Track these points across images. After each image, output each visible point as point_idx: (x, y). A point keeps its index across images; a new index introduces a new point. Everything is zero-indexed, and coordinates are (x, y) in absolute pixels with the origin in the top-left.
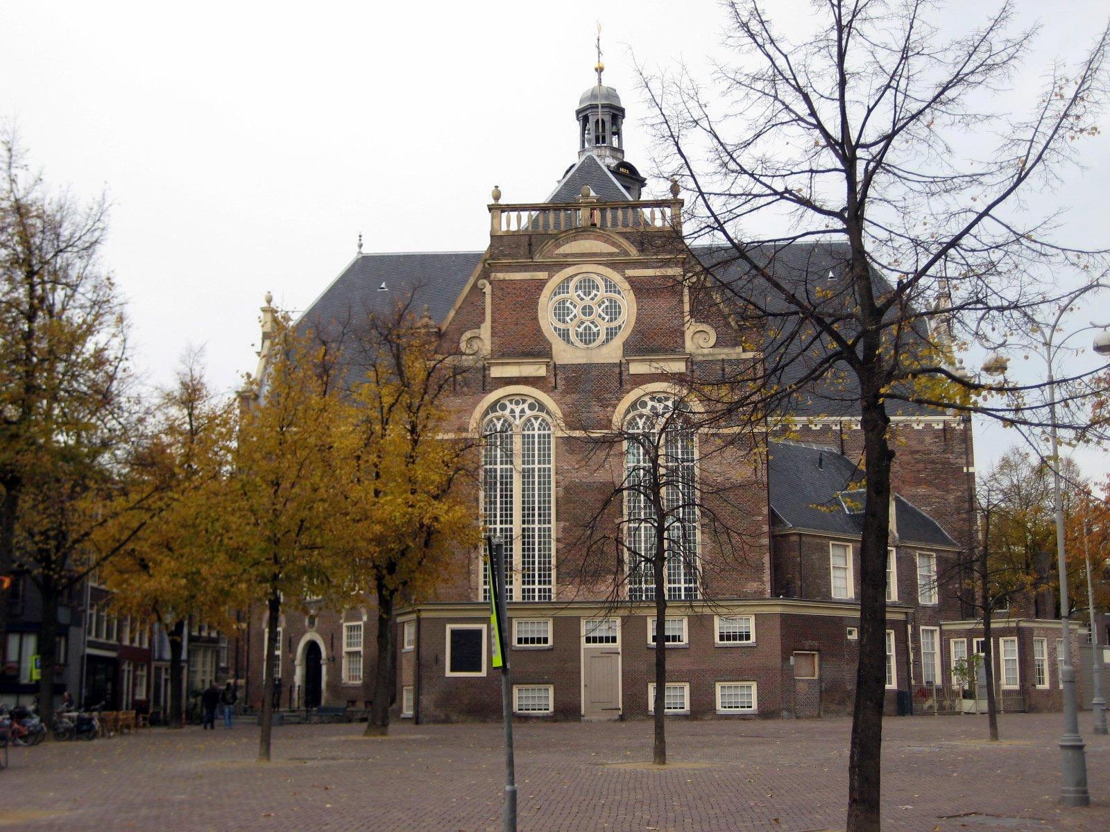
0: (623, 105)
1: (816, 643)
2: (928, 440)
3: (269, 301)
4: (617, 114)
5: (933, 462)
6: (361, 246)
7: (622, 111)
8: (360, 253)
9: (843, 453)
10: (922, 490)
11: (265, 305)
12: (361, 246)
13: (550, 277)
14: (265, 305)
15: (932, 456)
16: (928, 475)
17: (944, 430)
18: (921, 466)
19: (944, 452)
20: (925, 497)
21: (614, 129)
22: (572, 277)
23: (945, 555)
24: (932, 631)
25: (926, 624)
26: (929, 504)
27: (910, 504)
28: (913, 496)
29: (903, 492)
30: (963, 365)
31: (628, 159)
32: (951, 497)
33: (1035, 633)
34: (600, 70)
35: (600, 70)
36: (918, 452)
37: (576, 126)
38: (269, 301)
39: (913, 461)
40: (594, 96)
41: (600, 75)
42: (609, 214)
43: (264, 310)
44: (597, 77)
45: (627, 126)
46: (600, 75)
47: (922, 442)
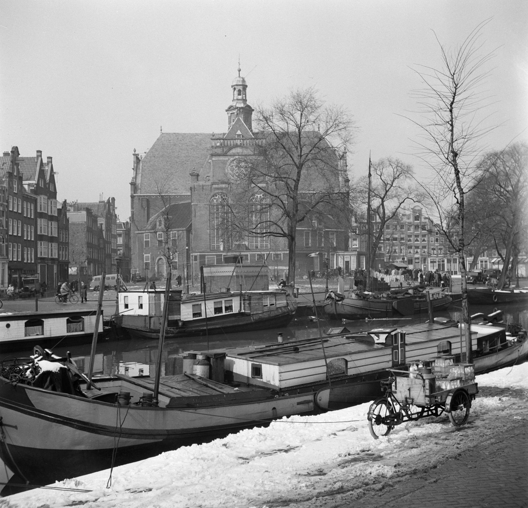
0: (247, 84)
3: (135, 151)
4: (245, 87)
6: (161, 130)
7: (247, 86)
11: (134, 153)
12: (161, 130)
14: (134, 153)
21: (244, 93)
22: (235, 159)
31: (248, 103)
34: (239, 71)
35: (239, 71)
37: (232, 90)
38: (135, 151)
42: (245, 141)
43: (134, 155)
45: (248, 90)
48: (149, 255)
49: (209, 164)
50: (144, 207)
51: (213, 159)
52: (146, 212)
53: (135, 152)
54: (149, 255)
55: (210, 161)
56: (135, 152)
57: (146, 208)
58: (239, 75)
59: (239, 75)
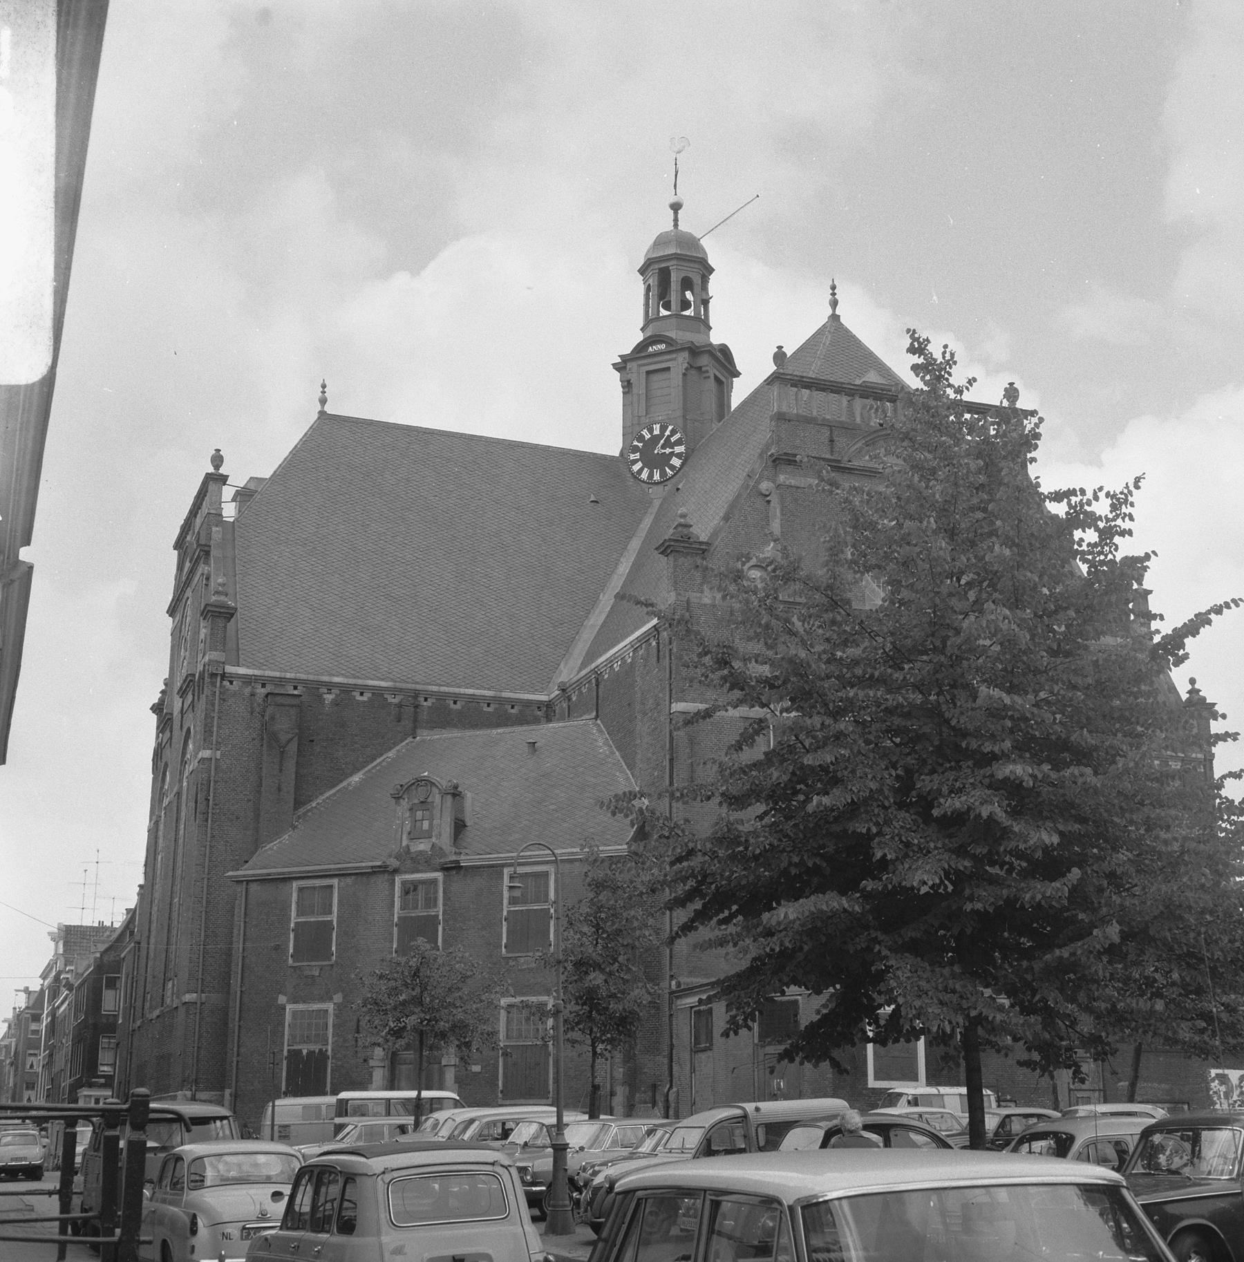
6: (323, 401)
7: (711, 270)
8: (322, 413)
12: (323, 401)
30: (1197, 686)
34: (676, 207)
35: (676, 207)
40: (660, 241)
41: (676, 213)
44: (672, 217)
46: (676, 213)
48: (330, 1007)
49: (759, 504)
50: (283, 738)
51: (782, 478)
52: (290, 765)
53: (217, 467)
54: (330, 1007)
55: (765, 486)
56: (217, 467)
57: (293, 747)
58: (676, 225)
59: (676, 225)
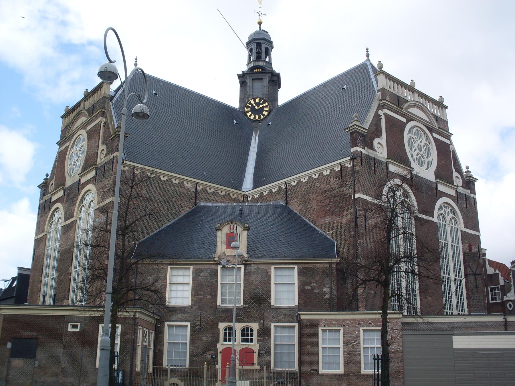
1: (35, 334)
2: (332, 180)
5: (335, 197)
9: (287, 203)
10: (327, 219)
13: (70, 143)
15: (334, 192)
16: (331, 207)
17: (341, 170)
18: (327, 201)
19: (341, 186)
20: (330, 223)
23: (306, 266)
24: (294, 327)
25: (278, 322)
26: (331, 229)
27: (320, 231)
28: (323, 225)
29: (317, 223)
32: (344, 220)
33: (322, 324)
34: (260, 23)
35: (260, 23)
36: (326, 191)
39: (324, 198)
47: (328, 183)
